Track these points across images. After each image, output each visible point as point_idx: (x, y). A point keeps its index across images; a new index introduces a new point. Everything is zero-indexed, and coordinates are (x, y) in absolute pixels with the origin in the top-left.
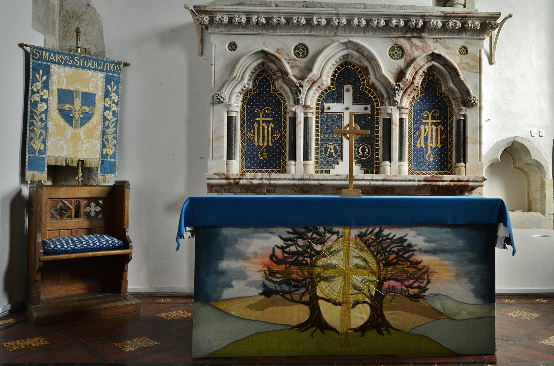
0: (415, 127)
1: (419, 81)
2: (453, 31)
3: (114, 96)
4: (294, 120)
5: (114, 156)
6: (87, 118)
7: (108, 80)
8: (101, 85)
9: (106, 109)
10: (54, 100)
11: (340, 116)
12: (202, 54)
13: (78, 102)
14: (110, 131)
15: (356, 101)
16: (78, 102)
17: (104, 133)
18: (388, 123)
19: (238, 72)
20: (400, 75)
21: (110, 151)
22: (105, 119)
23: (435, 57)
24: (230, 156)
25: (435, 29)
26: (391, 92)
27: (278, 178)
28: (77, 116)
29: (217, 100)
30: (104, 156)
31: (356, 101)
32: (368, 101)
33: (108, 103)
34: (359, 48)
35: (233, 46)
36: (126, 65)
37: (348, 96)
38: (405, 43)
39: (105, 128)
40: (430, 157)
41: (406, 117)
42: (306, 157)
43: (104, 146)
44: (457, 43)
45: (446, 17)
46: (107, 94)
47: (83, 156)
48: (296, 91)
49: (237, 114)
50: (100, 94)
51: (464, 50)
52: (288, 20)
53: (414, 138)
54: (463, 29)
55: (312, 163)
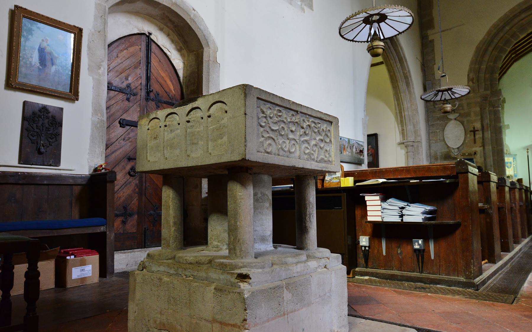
3: (515, 162)
5: (516, 174)
6: (511, 166)
7: (514, 159)
8: (512, 160)
9: (514, 164)
13: (509, 164)
14: (515, 169)
16: (509, 164)
17: (514, 169)
21: (515, 173)
22: (514, 167)
28: (509, 166)
30: (514, 174)
33: (514, 163)
36: (516, 155)
39: (514, 168)
43: (514, 172)
46: (514, 161)
47: (511, 174)
50: (512, 161)
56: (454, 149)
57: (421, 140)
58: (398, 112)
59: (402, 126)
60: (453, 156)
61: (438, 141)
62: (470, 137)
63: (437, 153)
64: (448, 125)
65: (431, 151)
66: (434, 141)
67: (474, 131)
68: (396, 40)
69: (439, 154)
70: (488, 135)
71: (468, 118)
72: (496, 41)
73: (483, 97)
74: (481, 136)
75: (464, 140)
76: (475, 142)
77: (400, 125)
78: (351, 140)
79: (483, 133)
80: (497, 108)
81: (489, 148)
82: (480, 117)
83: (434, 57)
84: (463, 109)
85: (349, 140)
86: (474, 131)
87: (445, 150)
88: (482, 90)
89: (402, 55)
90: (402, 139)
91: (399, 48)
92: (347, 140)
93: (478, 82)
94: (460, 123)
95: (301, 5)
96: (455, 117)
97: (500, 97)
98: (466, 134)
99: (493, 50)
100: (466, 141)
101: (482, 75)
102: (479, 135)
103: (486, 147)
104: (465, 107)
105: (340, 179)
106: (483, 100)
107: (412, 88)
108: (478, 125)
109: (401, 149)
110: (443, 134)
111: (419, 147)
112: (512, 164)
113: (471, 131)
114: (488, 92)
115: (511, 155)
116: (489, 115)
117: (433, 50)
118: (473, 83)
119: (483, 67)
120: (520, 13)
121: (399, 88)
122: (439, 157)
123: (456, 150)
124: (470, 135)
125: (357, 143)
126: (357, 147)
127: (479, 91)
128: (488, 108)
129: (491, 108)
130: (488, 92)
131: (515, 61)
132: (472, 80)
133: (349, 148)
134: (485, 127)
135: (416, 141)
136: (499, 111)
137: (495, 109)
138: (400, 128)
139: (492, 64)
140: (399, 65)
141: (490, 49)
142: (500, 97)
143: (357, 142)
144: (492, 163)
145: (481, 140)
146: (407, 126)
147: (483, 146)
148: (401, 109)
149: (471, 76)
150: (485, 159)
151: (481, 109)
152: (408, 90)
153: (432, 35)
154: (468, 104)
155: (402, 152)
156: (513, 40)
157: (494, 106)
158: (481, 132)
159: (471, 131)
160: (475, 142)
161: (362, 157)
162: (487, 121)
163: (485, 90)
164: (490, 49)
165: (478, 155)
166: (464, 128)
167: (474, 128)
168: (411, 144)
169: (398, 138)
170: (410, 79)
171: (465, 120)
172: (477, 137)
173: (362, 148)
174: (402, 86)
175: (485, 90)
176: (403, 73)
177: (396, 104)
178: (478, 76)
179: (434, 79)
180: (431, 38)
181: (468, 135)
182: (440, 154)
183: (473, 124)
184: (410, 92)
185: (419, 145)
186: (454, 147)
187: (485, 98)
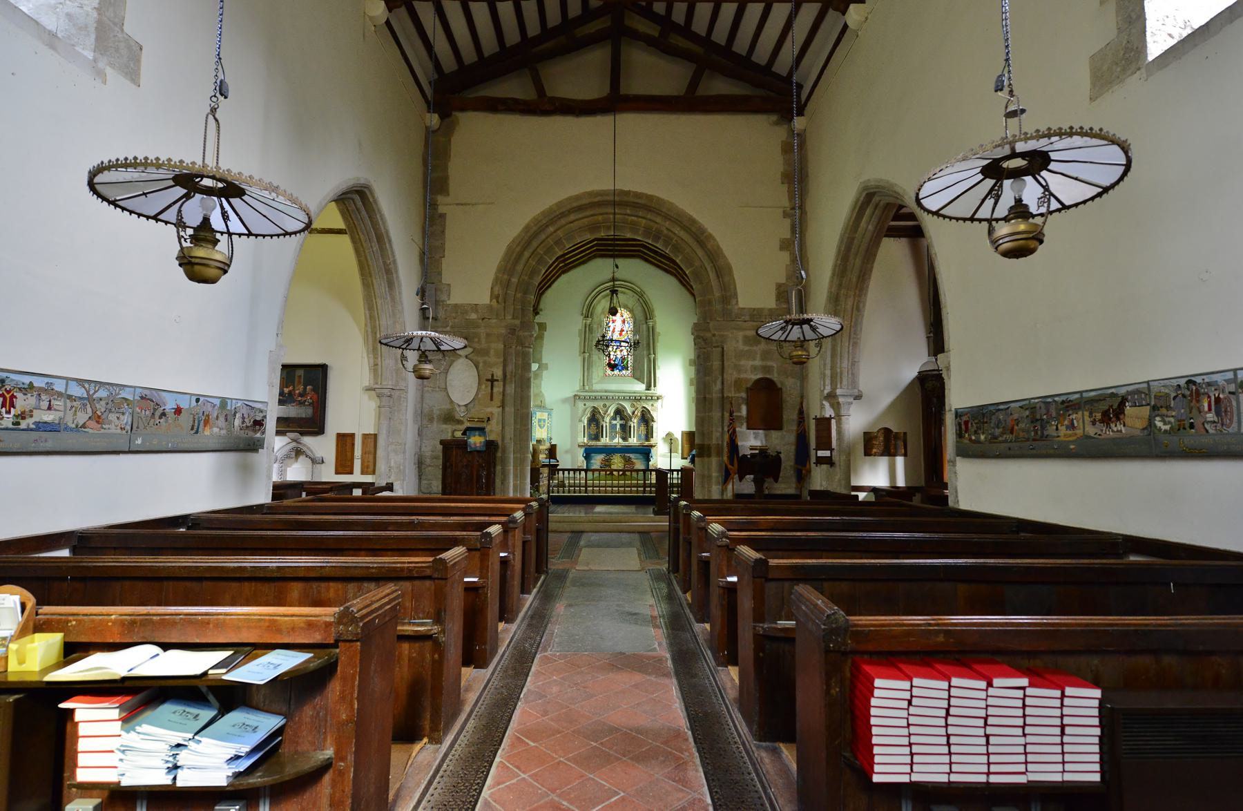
0: (638, 428)
1: (639, 414)
2: (649, 400)
4: (602, 426)
6: (544, 426)
10: (537, 422)
11: (616, 424)
12: (574, 405)
15: (621, 419)
18: (630, 427)
19: (586, 412)
20: (633, 413)
23: (645, 407)
24: (584, 437)
25: (643, 400)
26: (631, 418)
27: (599, 443)
29: (580, 421)
31: (621, 419)
32: (624, 420)
34: (621, 405)
35: (585, 405)
37: (618, 419)
38: (634, 403)
40: (643, 437)
41: (635, 425)
42: (606, 437)
44: (651, 403)
45: (647, 396)
48: (603, 418)
49: (586, 425)
51: (652, 405)
52: (601, 397)
53: (638, 431)
54: (652, 399)
55: (608, 439)
56: (459, 405)
57: (407, 387)
58: (370, 330)
59: (375, 358)
60: (457, 417)
61: (437, 389)
62: (486, 388)
63: (433, 411)
64: (455, 364)
65: (424, 405)
66: (430, 389)
67: (492, 381)
68: (371, 200)
69: (436, 412)
70: (511, 389)
71: (486, 358)
72: (535, 244)
73: (510, 329)
74: (501, 390)
75: (477, 394)
76: (492, 399)
77: (371, 356)
78: (229, 401)
79: (504, 386)
80: (527, 349)
81: (510, 410)
82: (502, 360)
83: (443, 244)
84: (479, 342)
85: (224, 401)
86: (492, 381)
87: (446, 406)
88: (509, 317)
89: (383, 231)
90: (372, 382)
91: (378, 216)
92: (217, 402)
93: (505, 302)
94: (472, 364)
95: (95, 60)
96: (468, 353)
97: (533, 333)
98: (480, 384)
99: (530, 257)
100: (480, 396)
101: (511, 292)
102: (498, 388)
103: (507, 409)
104: (483, 341)
105: (7, 647)
106: (509, 333)
107: (397, 294)
108: (498, 373)
109: (370, 398)
110: (446, 378)
111: (402, 399)
112: (546, 422)
113: (487, 380)
114: (517, 322)
115: (546, 409)
116: (515, 358)
117: (443, 232)
118: (498, 302)
119: (515, 280)
120: (563, 215)
121: (373, 289)
122: (435, 416)
123: (463, 409)
124: (486, 387)
125: (246, 405)
126: (246, 416)
127: (504, 316)
128: (514, 347)
129: (519, 348)
130: (517, 322)
131: (564, 272)
132: (497, 297)
133: (222, 419)
134: (508, 377)
135: (398, 388)
136: (529, 352)
137: (524, 349)
138: (372, 361)
139: (526, 278)
140: (376, 248)
141: (527, 254)
142: (533, 333)
143: (246, 403)
144: (512, 436)
145: (501, 397)
146: (383, 359)
147: (503, 406)
148: (375, 327)
149: (496, 289)
150: (503, 427)
151: (505, 346)
152: (390, 294)
153: (445, 205)
154: (488, 335)
155: (370, 405)
156: (556, 249)
157: (522, 345)
158: (501, 383)
159: (487, 380)
160: (492, 399)
161: (258, 435)
162: (510, 368)
163: (513, 318)
164: (527, 254)
165: (494, 422)
166: (478, 373)
167: (493, 375)
168: (387, 392)
169: (366, 379)
170: (395, 275)
171: (481, 360)
172: (495, 390)
173: (261, 415)
174: (380, 285)
175: (513, 318)
176: (384, 263)
177: (368, 315)
178: (506, 293)
179: (441, 281)
180: (441, 209)
181: (483, 387)
182: (438, 412)
183: (492, 370)
184: (393, 299)
185: (402, 396)
186: (460, 404)
187: (512, 331)
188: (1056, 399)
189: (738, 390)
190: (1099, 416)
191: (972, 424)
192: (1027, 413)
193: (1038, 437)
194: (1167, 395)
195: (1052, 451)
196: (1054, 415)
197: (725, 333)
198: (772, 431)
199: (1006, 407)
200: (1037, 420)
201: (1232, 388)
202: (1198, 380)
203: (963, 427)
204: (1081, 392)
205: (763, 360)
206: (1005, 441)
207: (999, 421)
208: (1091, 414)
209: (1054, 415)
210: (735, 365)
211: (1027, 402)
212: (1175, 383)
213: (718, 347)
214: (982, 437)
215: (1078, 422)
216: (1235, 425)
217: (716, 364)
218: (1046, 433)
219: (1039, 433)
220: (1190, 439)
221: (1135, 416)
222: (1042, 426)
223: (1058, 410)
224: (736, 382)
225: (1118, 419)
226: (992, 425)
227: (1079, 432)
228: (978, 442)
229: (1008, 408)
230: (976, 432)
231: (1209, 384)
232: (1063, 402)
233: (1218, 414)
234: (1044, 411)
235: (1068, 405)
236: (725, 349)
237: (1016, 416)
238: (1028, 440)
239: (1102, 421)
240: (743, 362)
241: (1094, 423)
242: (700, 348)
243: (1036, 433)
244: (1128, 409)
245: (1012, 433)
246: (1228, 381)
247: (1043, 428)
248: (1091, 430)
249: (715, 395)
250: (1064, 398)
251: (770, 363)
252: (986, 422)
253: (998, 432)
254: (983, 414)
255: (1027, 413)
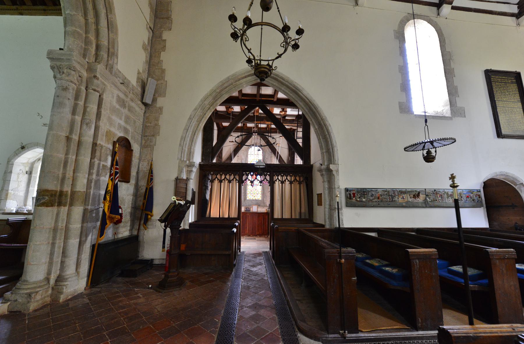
188: (397, 190)
189: (108, 141)
190: (412, 196)
191: (357, 194)
192: (386, 193)
193: (390, 201)
194: (430, 193)
195: (397, 205)
196: (397, 194)
197: (106, 83)
198: (123, 183)
199: (376, 190)
200: (390, 195)
201: (443, 193)
202: (437, 190)
203: (352, 195)
204: (406, 189)
205: (126, 122)
206: (376, 202)
207: (373, 195)
208: (410, 195)
209: (397, 194)
210: (109, 117)
211: (386, 189)
212: (432, 190)
213: (98, 92)
214: (364, 200)
215: (405, 197)
216: (445, 200)
217: (93, 108)
218: (394, 200)
219: (391, 200)
220: (436, 203)
221: (422, 197)
222: (392, 197)
223: (398, 194)
224: (107, 132)
225: (418, 197)
226: (369, 195)
227: (406, 200)
228: (362, 201)
229: (377, 190)
230: (359, 198)
231: (439, 191)
232: (400, 191)
233: (441, 198)
234: (392, 193)
235: (402, 192)
236: (104, 96)
237: (380, 193)
238: (387, 201)
239: (413, 197)
240: (114, 117)
241: (411, 198)
242: (71, 82)
243: (390, 200)
244: (421, 195)
245: (379, 198)
246: (443, 191)
247: (392, 198)
248: (410, 200)
249: (88, 138)
250: (400, 190)
251: (128, 127)
252: (366, 194)
253: (371, 198)
254: (364, 192)
255: (386, 193)
